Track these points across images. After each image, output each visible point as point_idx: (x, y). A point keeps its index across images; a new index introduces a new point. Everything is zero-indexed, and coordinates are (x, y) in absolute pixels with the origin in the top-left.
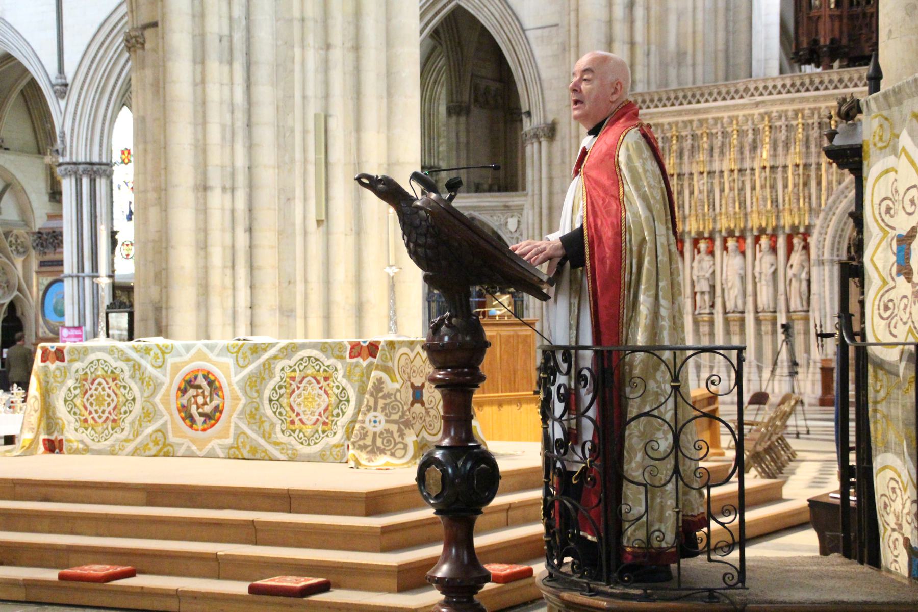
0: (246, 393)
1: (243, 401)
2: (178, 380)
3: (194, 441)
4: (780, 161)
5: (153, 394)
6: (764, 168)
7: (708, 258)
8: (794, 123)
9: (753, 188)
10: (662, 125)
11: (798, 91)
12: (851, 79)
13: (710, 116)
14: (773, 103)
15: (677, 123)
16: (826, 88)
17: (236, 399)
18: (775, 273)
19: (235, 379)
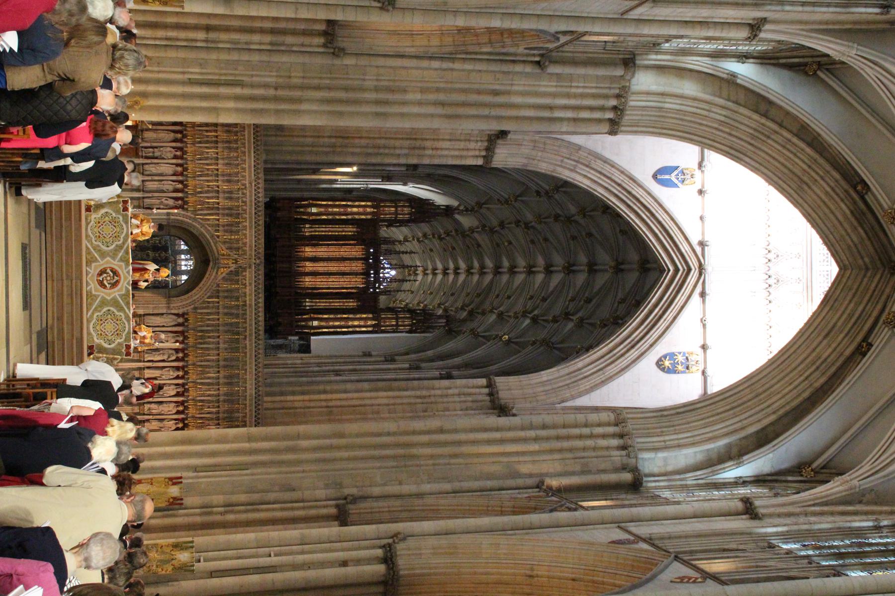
0: (112, 299)
1: (109, 298)
2: (116, 268)
3: (93, 276)
4: (221, 195)
5: (110, 257)
6: (218, 187)
7: (172, 155)
8: (240, 201)
9: (208, 181)
10: (244, 131)
11: (255, 204)
12: (259, 230)
13: (247, 158)
14: (251, 192)
15: (244, 139)
16: (255, 218)
17: (109, 295)
18: (163, 191)
19: (116, 294)
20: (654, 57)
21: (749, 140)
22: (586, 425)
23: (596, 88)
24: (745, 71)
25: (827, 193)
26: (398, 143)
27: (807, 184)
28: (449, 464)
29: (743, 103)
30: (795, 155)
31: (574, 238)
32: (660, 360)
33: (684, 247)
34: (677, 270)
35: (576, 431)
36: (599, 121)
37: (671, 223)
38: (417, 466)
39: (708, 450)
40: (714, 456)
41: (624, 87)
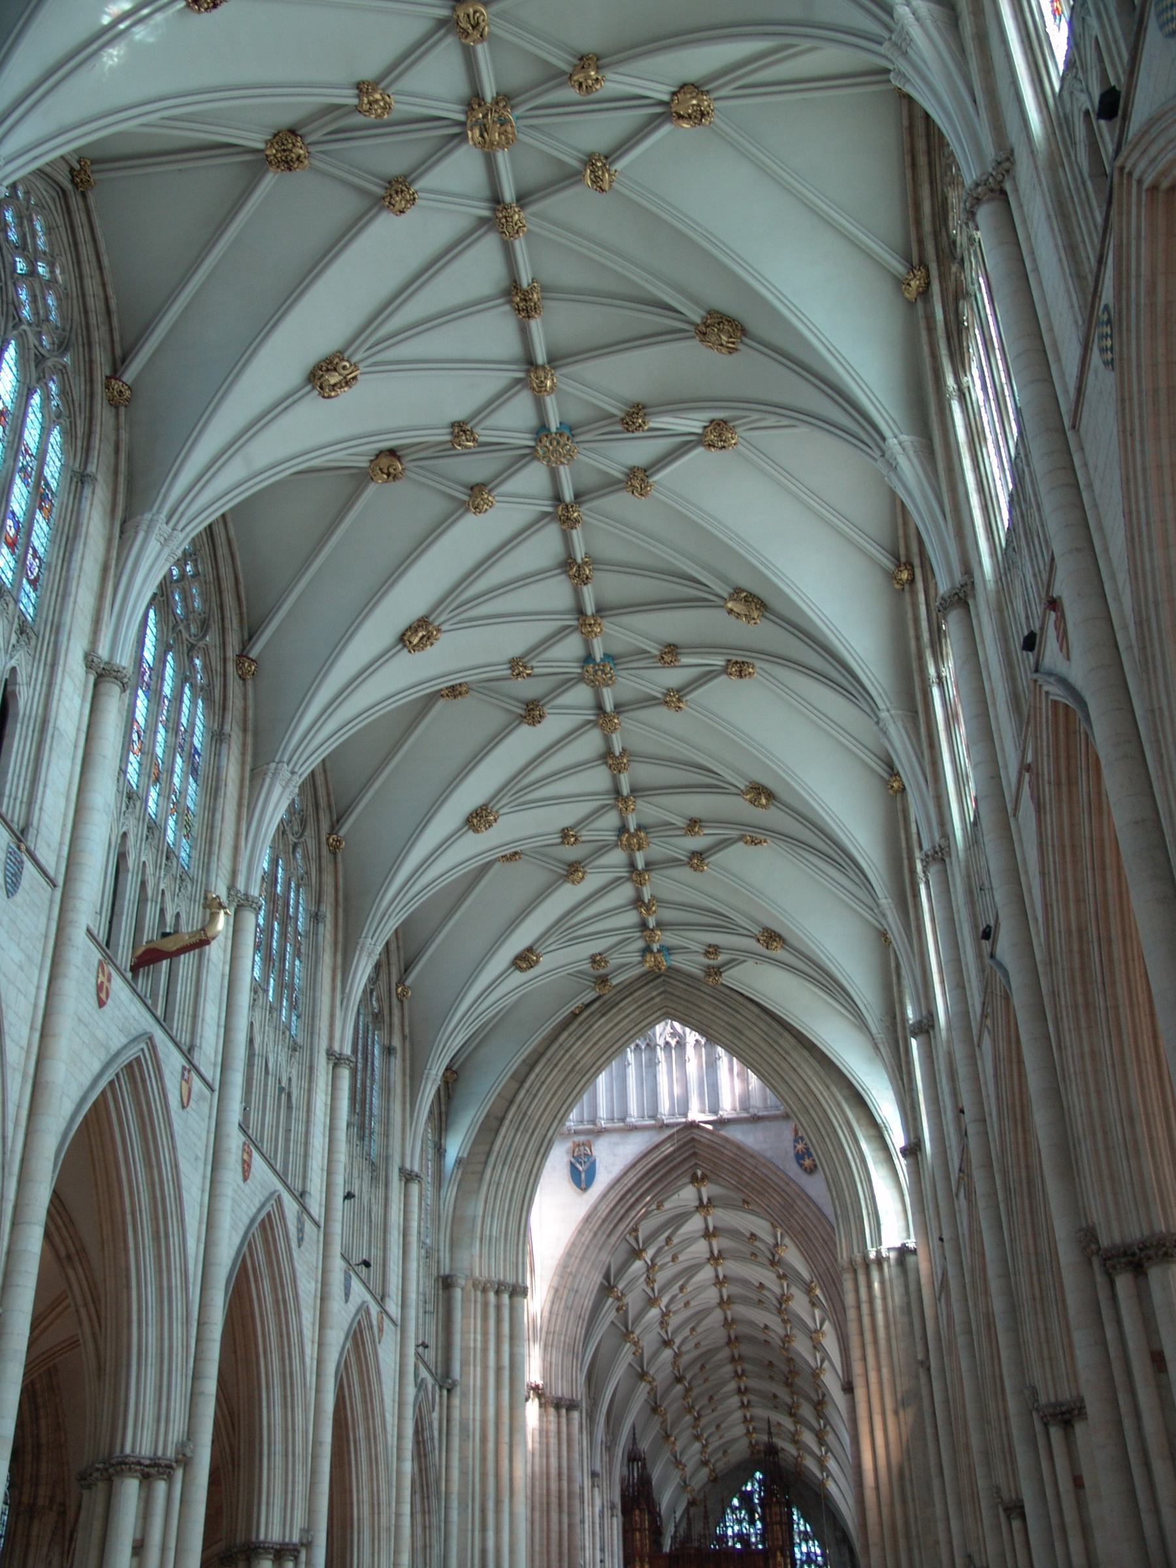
20: (442, 1254)
21: (528, 1136)
22: (859, 1308)
23: (475, 1318)
24: (455, 1147)
25: (584, 1043)
26: (554, 1527)
27: (575, 1066)
28: (911, 1480)
29: (487, 1148)
30: (543, 1083)
31: (674, 1258)
32: (805, 1170)
33: (668, 1149)
34: (695, 1154)
35: (866, 1320)
36: (512, 1309)
37: (639, 1167)
38: (916, 1521)
39: (875, 1163)
40: (881, 1155)
41: (475, 1286)
